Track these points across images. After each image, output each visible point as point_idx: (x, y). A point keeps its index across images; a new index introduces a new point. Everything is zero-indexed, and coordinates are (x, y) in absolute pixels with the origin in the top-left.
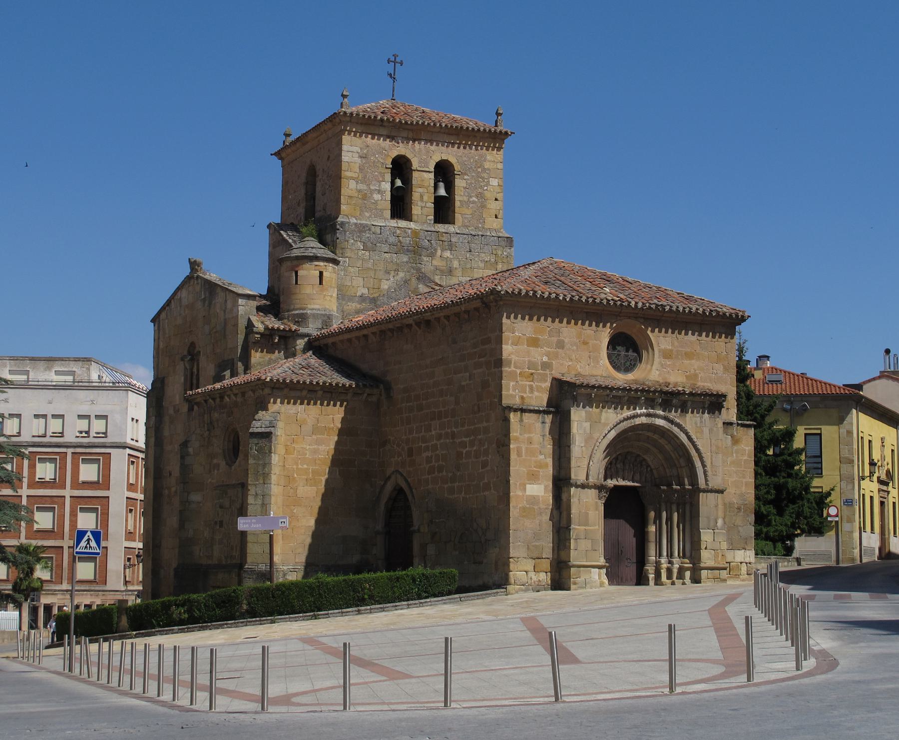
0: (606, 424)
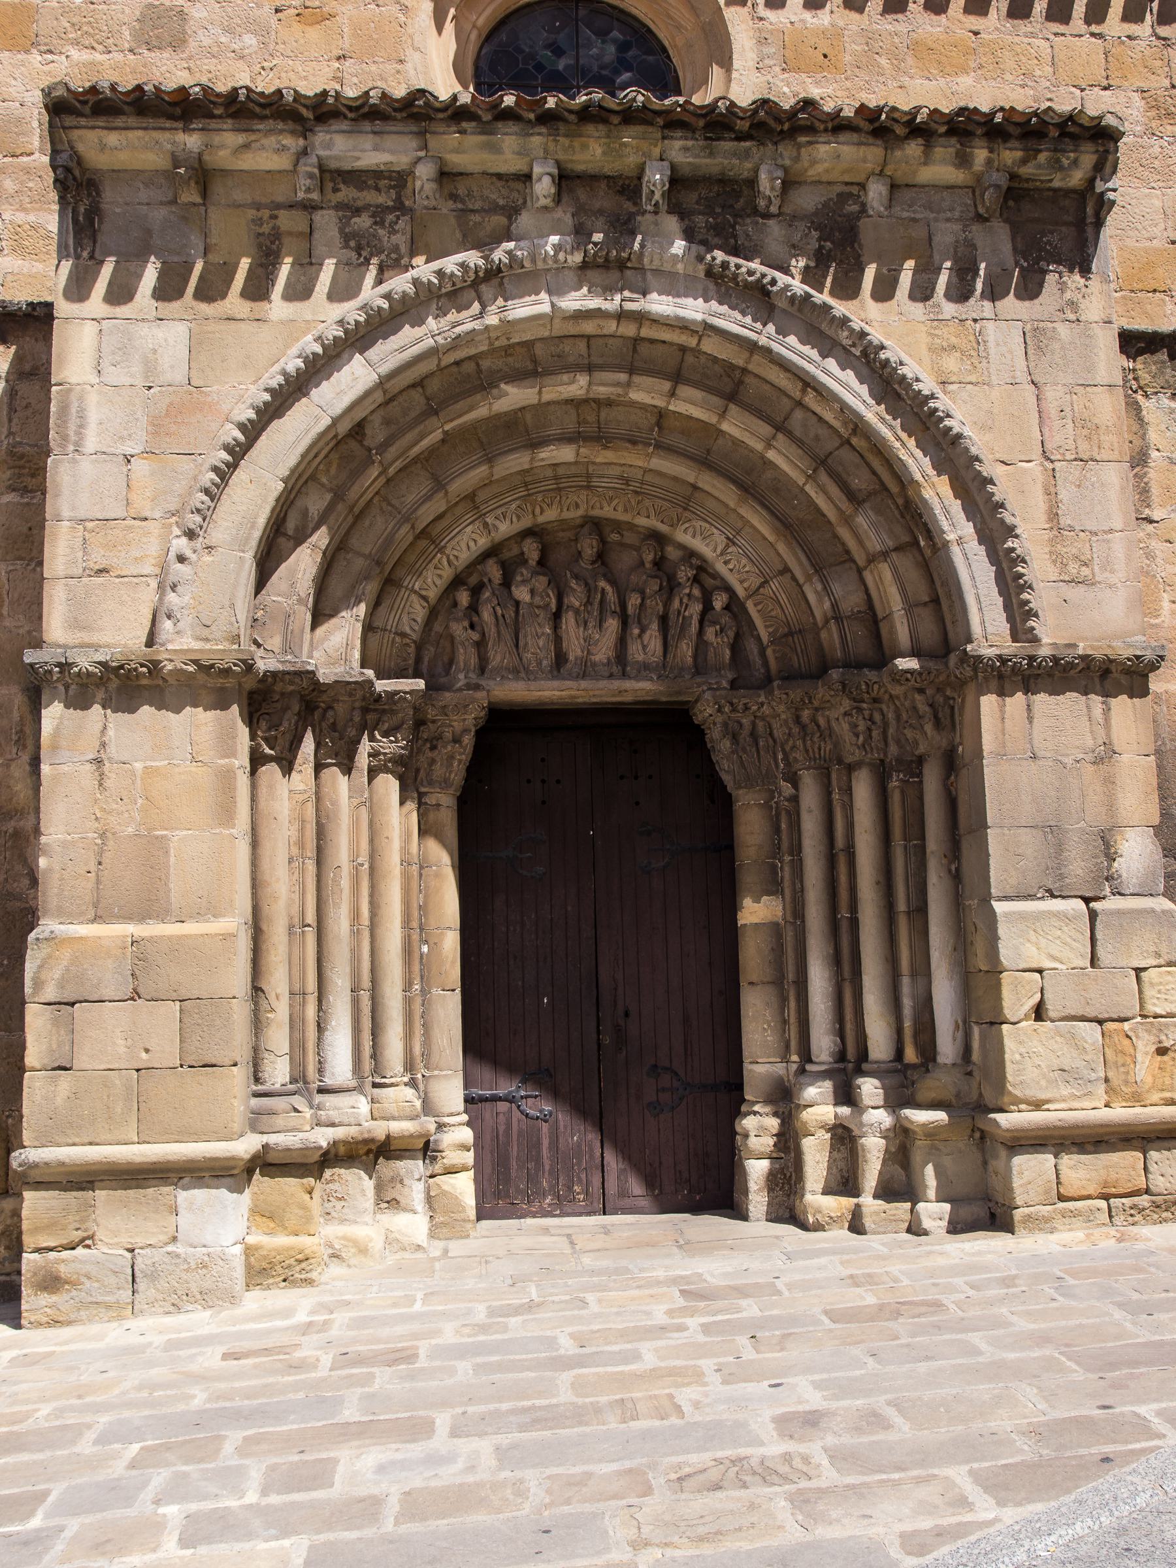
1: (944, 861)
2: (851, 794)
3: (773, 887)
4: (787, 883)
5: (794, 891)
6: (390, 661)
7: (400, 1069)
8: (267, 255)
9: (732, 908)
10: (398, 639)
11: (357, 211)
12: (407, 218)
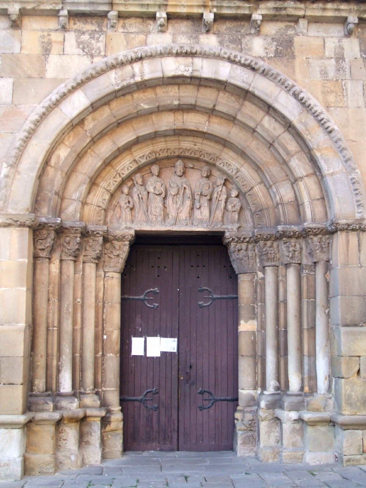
0: (56, 81)
1: (323, 309)
2: (286, 278)
3: (253, 316)
4: (259, 314)
5: (262, 318)
6: (93, 218)
7: (92, 387)
8: (46, 51)
9: (236, 324)
10: (97, 208)
11: (84, 33)
12: (104, 36)
